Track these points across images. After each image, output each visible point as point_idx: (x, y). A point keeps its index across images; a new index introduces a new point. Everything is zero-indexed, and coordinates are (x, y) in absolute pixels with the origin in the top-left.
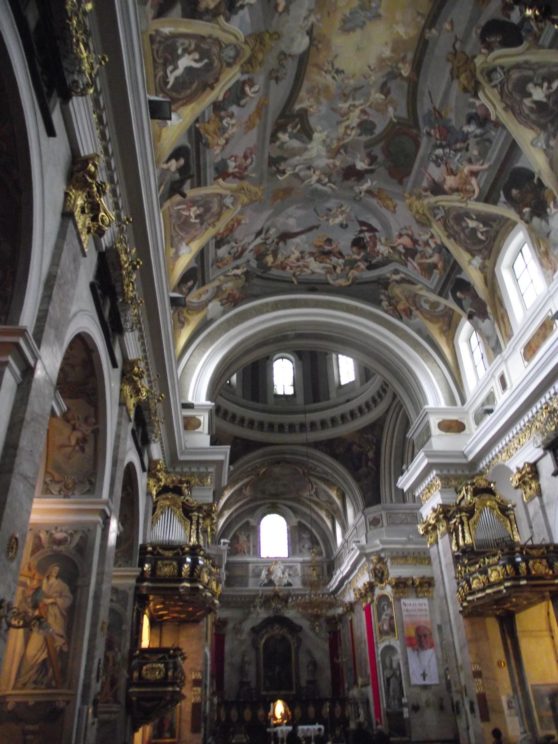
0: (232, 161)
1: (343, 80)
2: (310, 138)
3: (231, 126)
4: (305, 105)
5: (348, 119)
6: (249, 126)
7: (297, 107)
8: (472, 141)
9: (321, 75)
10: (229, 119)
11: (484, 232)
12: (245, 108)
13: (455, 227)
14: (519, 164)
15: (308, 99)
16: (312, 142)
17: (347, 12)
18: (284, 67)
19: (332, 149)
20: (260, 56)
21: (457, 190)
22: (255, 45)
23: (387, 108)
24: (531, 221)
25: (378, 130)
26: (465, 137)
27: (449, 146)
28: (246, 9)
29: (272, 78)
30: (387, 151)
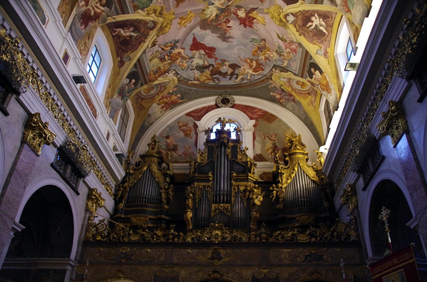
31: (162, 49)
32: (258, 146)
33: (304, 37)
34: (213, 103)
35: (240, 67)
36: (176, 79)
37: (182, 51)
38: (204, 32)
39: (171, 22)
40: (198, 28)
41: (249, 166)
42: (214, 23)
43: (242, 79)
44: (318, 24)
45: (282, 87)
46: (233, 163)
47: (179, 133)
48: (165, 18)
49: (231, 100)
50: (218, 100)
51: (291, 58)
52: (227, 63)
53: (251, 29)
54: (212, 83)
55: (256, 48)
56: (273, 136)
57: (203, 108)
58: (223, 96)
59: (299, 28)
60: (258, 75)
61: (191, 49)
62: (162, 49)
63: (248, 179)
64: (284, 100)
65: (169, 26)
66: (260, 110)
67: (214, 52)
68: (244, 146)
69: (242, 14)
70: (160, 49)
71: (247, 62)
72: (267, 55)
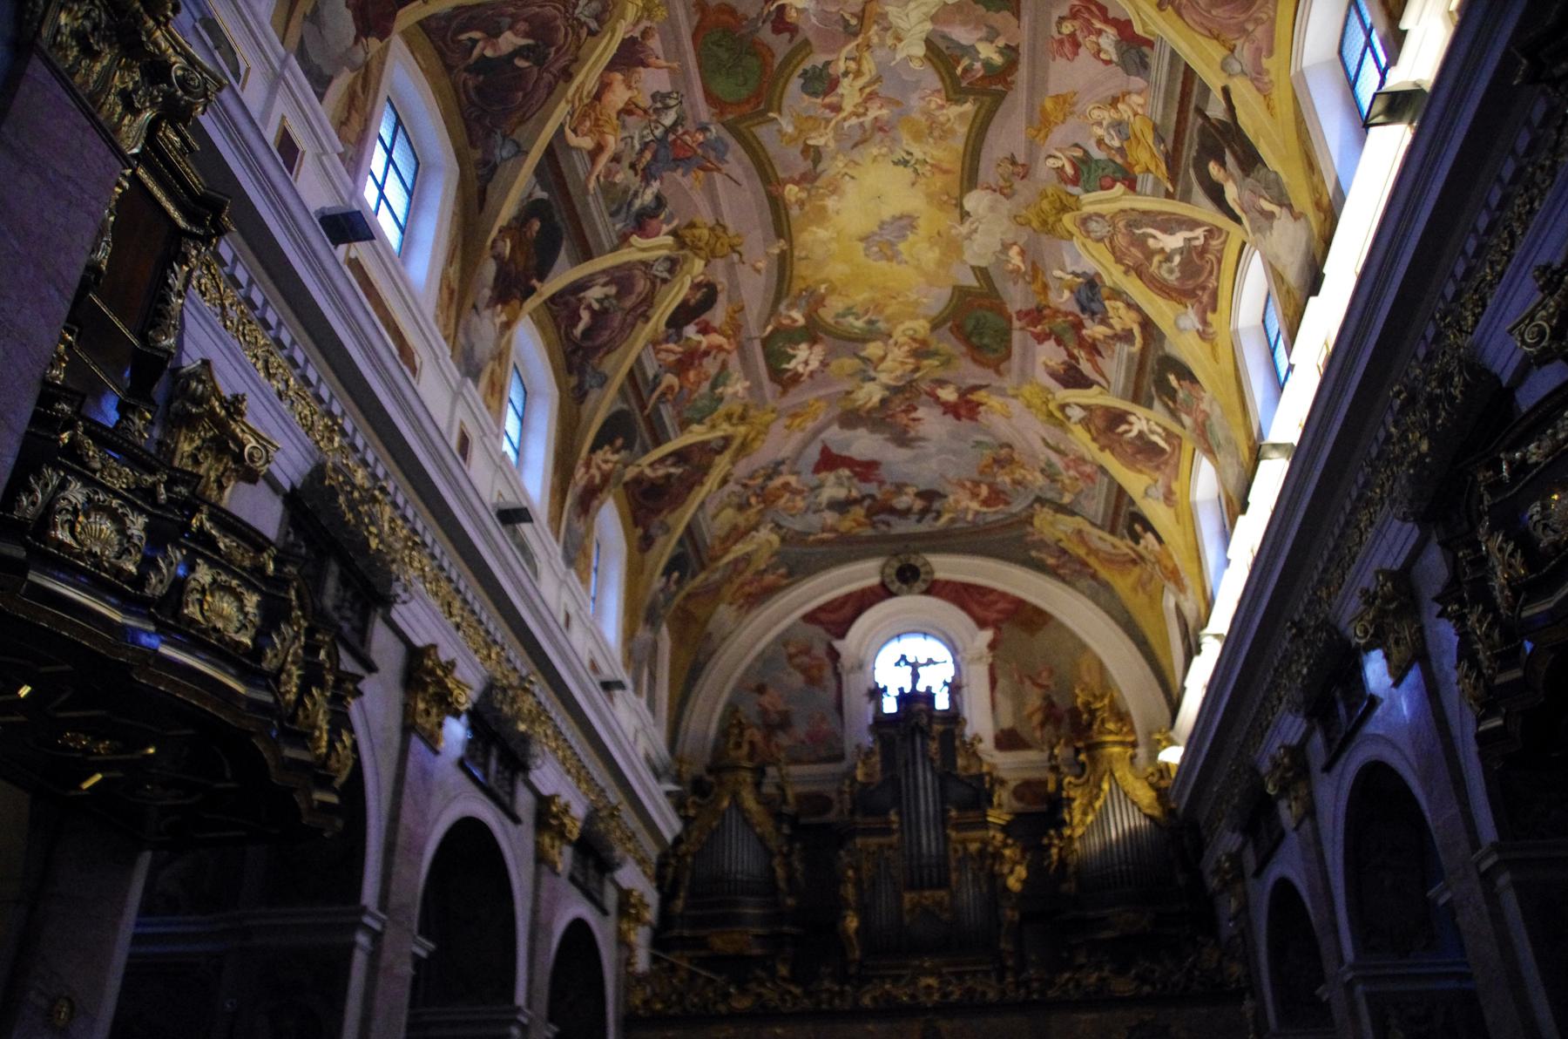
0: (1106, 52)
1: (892, 152)
2: (929, 43)
3: (1105, 123)
4: (954, 111)
5: (861, 90)
6: (1066, 102)
7: (968, 107)
8: (635, 182)
9: (932, 158)
10: (1107, 141)
11: (473, 47)
12: (1072, 141)
13: (537, 10)
14: (563, 256)
15: (949, 120)
16: (924, 35)
17: (911, 237)
18: (1001, 175)
19: (875, 22)
20: (1045, 205)
21: (598, 97)
22: (1054, 223)
23: (796, 127)
24: (495, 257)
25: (795, 84)
26: (647, 176)
27: (661, 141)
28: (1070, 269)
29: (1023, 165)
30: (760, 52)
31: (745, 486)
32: (1005, 706)
33: (1113, 452)
34: (875, 580)
35: (945, 496)
36: (775, 539)
37: (792, 480)
38: (847, 433)
39: (767, 426)
40: (835, 428)
41: (987, 786)
42: (875, 415)
43: (952, 521)
44: (1145, 429)
45: (1061, 544)
46: (946, 776)
47: (789, 674)
48: (751, 424)
49: (922, 570)
50: (888, 571)
51: (1082, 491)
52: (911, 490)
53: (974, 423)
54: (868, 532)
55: (987, 460)
56: (1045, 674)
57: (849, 597)
58: (902, 557)
59: (1099, 434)
60: (996, 512)
61: (818, 469)
62: (745, 486)
63: (987, 822)
64: (1067, 571)
65: (761, 437)
66: (1004, 595)
67: (877, 468)
68: (969, 732)
69: (948, 394)
70: (738, 488)
71: (963, 486)
72: (1017, 476)
